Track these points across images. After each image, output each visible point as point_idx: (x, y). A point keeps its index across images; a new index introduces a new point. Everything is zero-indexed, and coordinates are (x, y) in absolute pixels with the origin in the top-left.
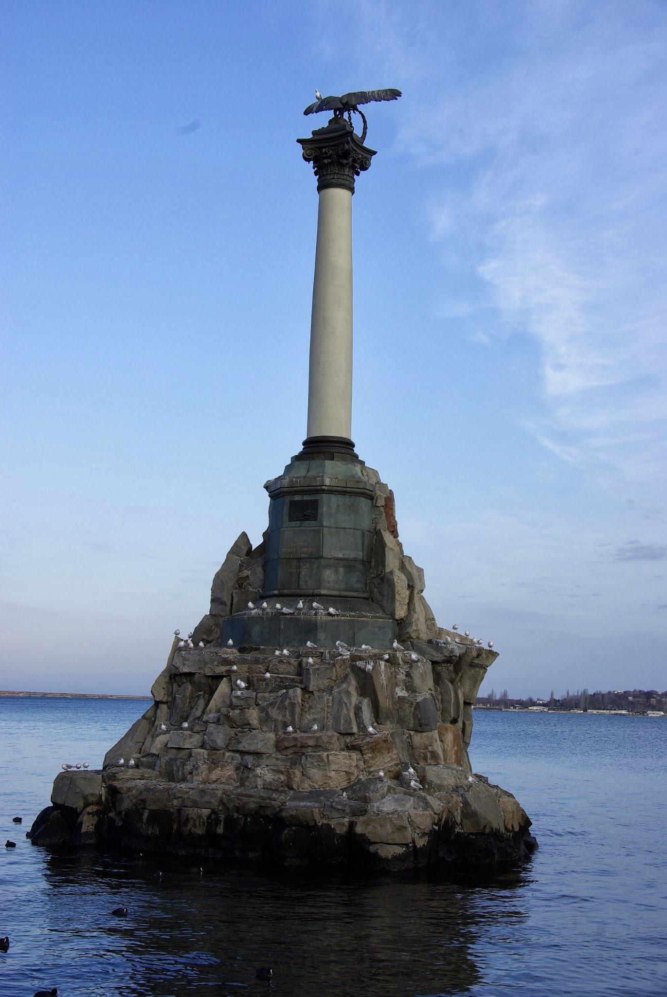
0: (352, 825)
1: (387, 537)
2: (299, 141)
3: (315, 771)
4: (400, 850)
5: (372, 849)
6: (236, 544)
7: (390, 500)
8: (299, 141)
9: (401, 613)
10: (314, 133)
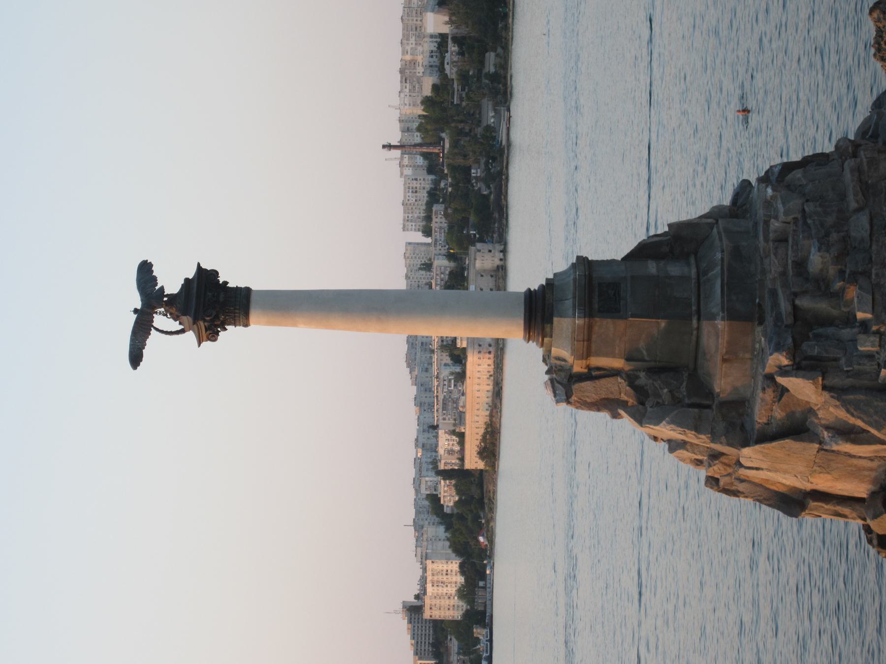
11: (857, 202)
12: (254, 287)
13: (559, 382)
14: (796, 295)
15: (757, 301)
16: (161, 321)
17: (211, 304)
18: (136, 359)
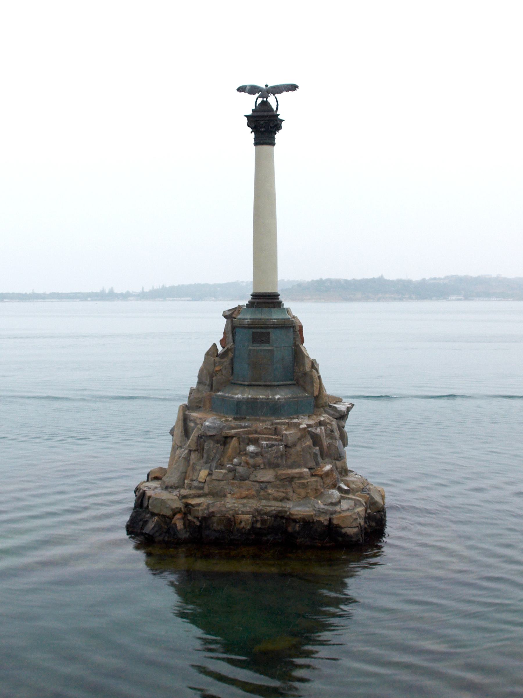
0: (330, 520)
1: (301, 346)
2: (245, 116)
3: (300, 490)
4: (356, 530)
5: (343, 531)
6: (210, 350)
7: (301, 327)
8: (245, 116)
9: (316, 393)
10: (253, 110)
11: (280, 475)
12: (275, 147)
13: (233, 312)
14: (239, 438)
15: (248, 417)
16: (260, 100)
17: (265, 125)
18: (241, 89)
